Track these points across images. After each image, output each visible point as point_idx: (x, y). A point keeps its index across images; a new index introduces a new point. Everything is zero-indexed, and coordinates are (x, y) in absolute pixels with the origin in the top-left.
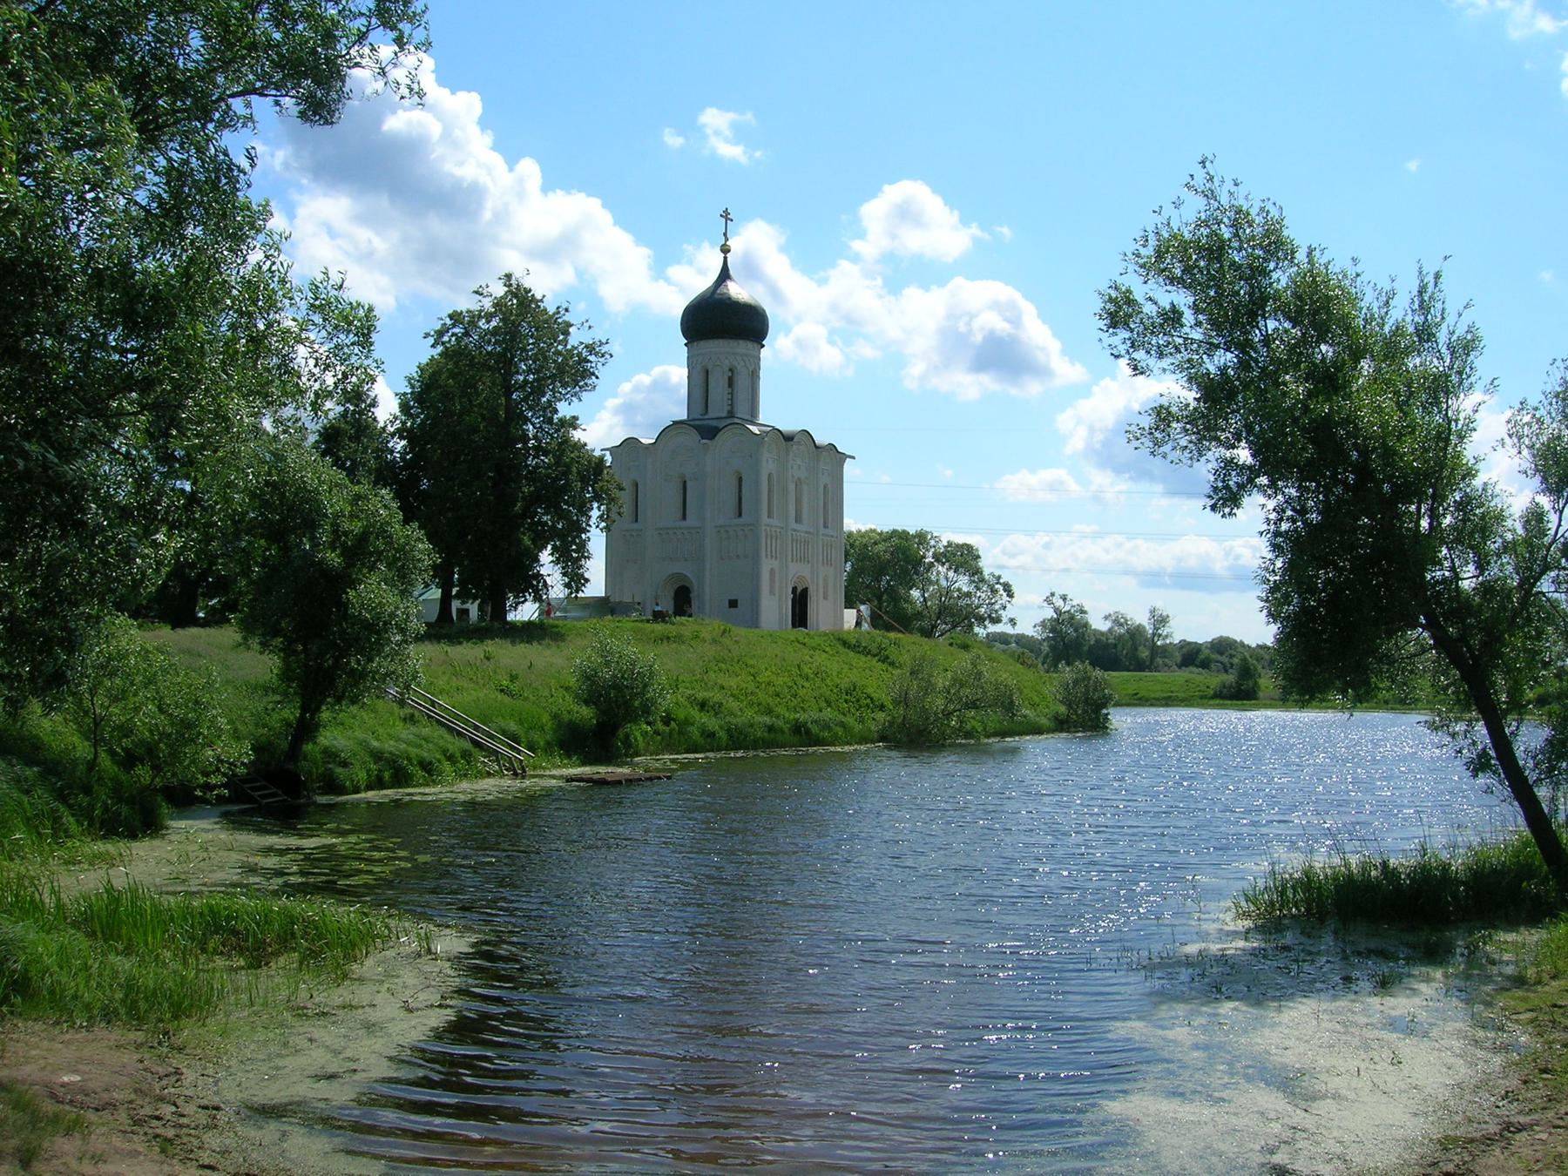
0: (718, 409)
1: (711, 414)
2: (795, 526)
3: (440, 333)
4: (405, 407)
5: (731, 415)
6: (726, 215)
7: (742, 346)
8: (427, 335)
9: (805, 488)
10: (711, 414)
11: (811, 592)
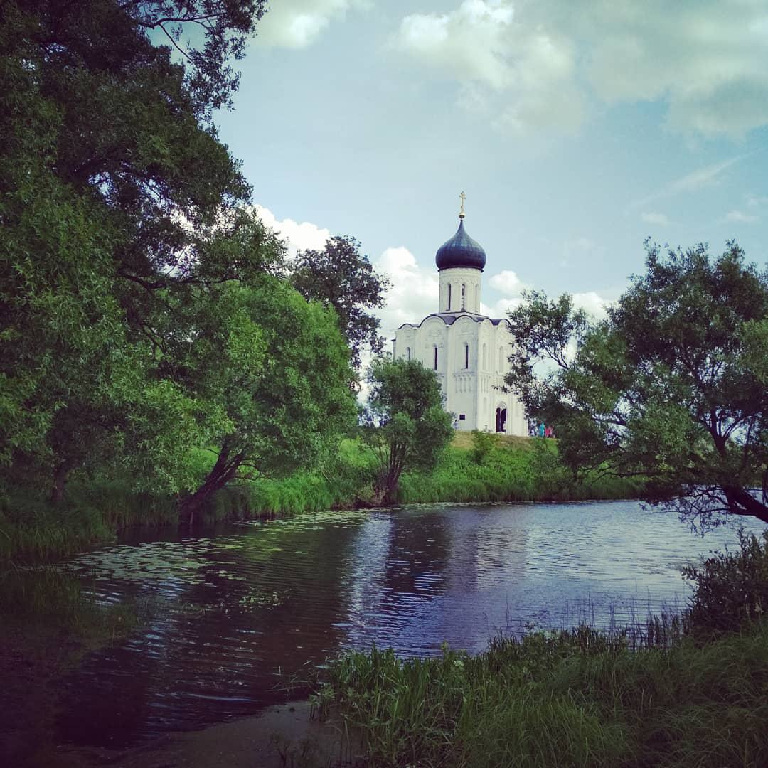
0: (456, 307)
1: (452, 311)
5: (463, 310)
6: (462, 195)
10: (452, 311)
11: (508, 412)
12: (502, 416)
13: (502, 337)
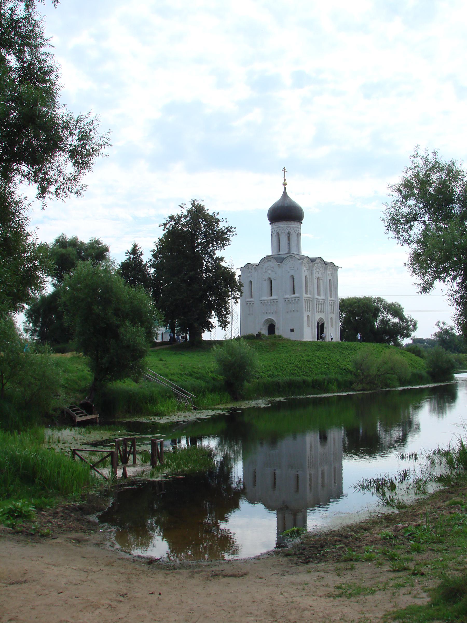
0: (284, 250)
3: (165, 224)
4: (155, 255)
5: (289, 252)
6: (284, 170)
7: (293, 224)
8: (160, 226)
9: (321, 281)
10: (281, 253)
11: (326, 325)
12: (321, 328)
13: (318, 270)
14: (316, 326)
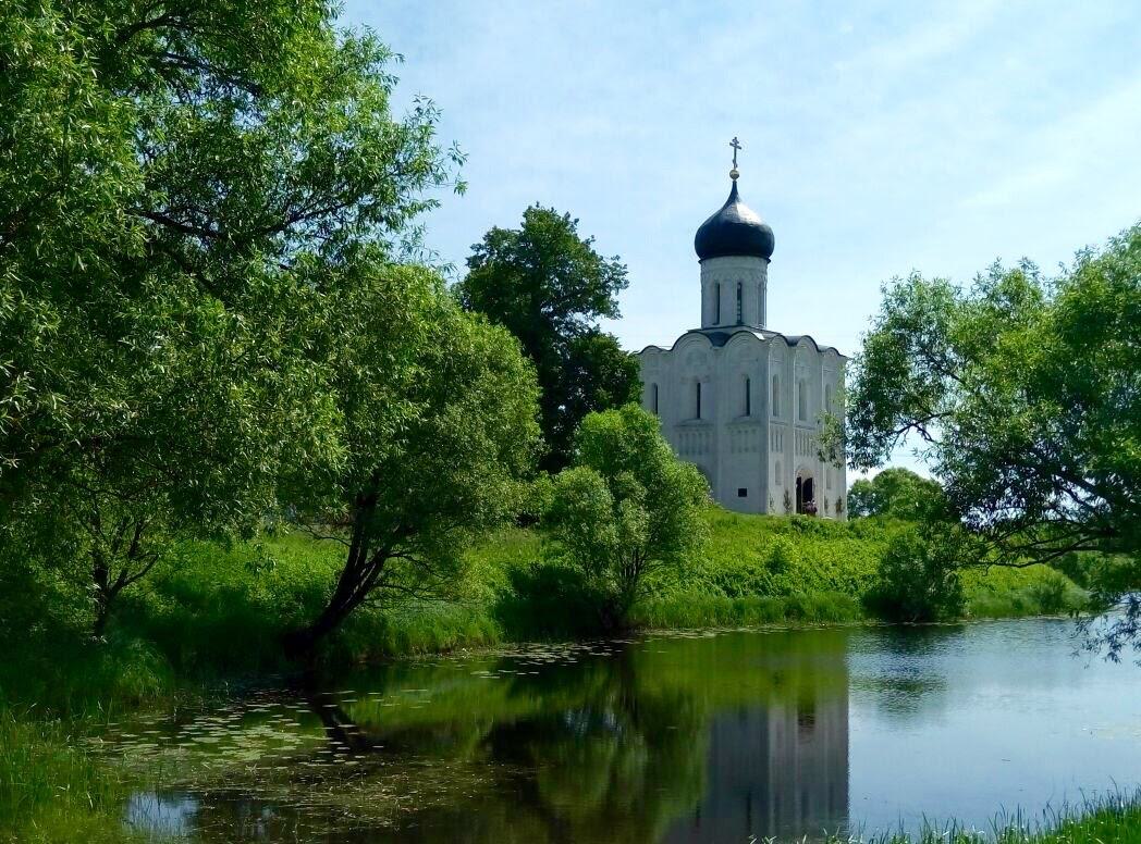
0: (729, 317)
2: (801, 423)
5: (740, 323)
6: (735, 144)
7: (749, 262)
9: (808, 387)
11: (815, 482)
14: (795, 486)
